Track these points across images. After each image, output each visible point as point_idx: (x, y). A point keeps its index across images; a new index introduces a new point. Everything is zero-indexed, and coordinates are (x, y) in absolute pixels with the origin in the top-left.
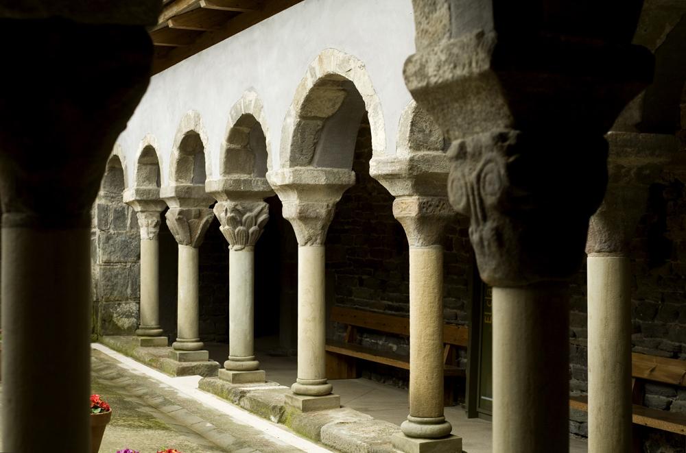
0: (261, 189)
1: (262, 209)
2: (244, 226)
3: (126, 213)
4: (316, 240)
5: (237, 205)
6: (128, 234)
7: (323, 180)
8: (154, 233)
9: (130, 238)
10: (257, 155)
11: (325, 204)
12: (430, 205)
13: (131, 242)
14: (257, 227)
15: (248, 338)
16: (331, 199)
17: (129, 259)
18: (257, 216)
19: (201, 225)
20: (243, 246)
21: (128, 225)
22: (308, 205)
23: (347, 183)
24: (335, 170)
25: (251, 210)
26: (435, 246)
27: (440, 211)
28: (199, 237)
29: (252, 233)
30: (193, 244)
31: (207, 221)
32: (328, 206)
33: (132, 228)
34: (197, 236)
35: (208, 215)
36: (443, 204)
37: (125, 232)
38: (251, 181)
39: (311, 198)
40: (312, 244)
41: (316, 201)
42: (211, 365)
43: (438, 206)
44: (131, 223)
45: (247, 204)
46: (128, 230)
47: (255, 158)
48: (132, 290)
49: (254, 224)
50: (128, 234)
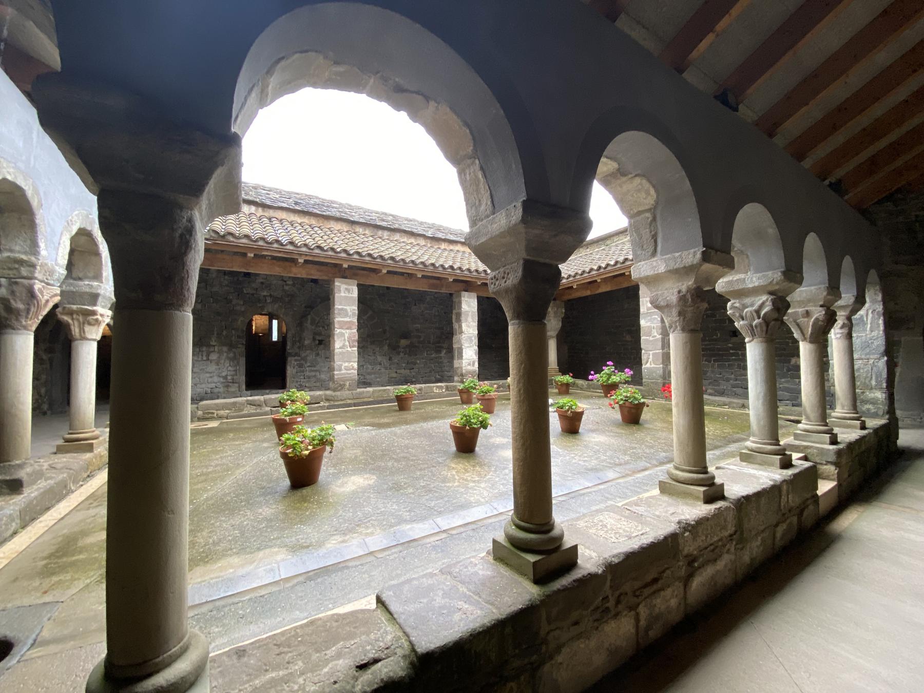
0: (756, 284)
1: (763, 304)
2: (747, 320)
3: (865, 319)
4: (676, 327)
5: (735, 303)
6: (868, 336)
7: (663, 268)
8: (842, 333)
9: (871, 339)
10: (749, 254)
11: (676, 290)
13: (872, 343)
14: (761, 319)
15: (762, 423)
16: (683, 285)
17: (872, 357)
18: (758, 312)
19: (811, 323)
20: (751, 339)
21: (868, 329)
22: (657, 294)
23: (690, 264)
24: (677, 254)
25: (752, 305)
27: (505, 282)
28: (811, 333)
29: (756, 326)
30: (808, 340)
31: (817, 319)
32: (679, 292)
33: (872, 331)
34: (809, 333)
35: (817, 313)
37: (864, 335)
38: (744, 279)
39: (660, 288)
40: (674, 331)
41: (666, 289)
44: (871, 327)
45: (747, 301)
46: (868, 333)
47: (747, 257)
48: (876, 382)
49: (756, 317)
50: (868, 336)
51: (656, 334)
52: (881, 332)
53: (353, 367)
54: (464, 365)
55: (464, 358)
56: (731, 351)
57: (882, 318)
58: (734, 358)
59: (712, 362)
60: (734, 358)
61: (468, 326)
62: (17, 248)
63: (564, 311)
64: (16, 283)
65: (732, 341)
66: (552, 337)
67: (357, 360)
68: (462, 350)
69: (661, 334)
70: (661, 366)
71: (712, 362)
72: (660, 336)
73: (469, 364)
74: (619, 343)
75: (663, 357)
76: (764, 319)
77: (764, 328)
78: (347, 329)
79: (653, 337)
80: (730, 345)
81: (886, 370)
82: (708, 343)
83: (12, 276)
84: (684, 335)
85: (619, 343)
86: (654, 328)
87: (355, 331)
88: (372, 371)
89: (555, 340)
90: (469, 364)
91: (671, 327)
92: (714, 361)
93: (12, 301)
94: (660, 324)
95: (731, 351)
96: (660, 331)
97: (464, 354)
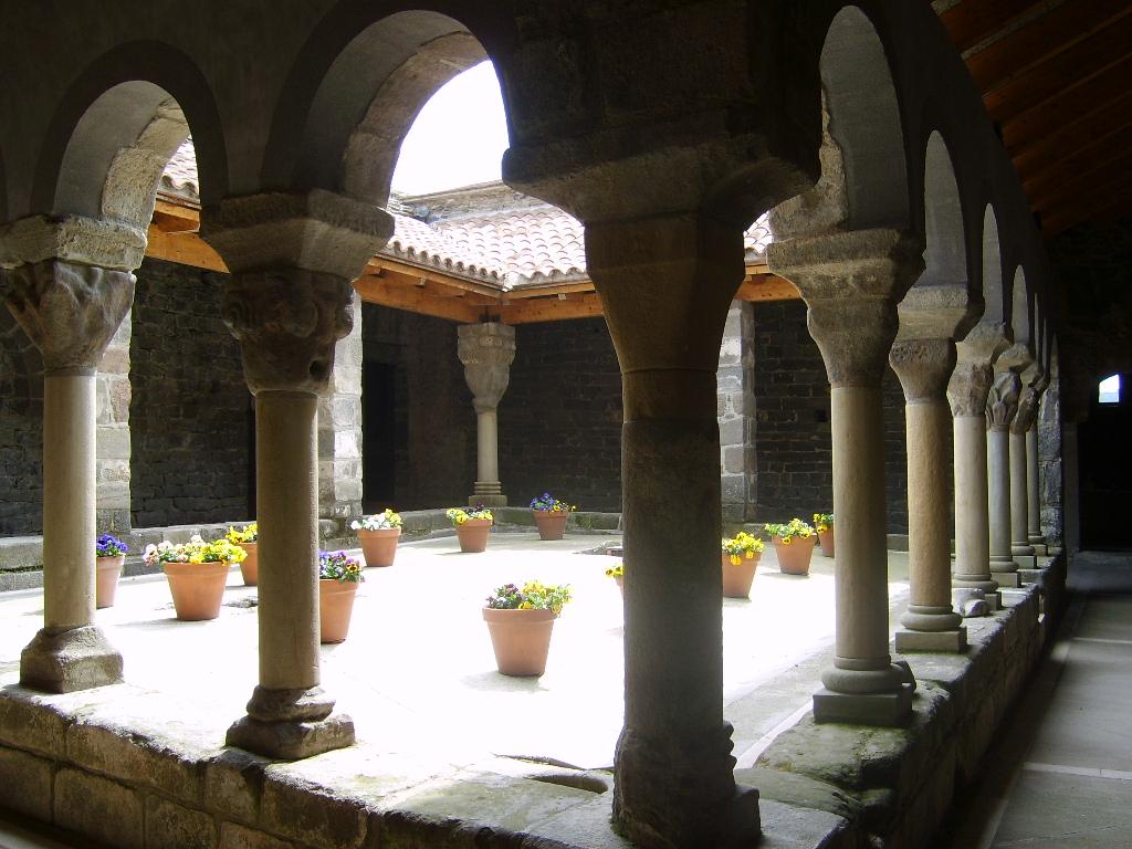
1: (1005, 381)
12: (906, 353)
26: (925, 399)
29: (996, 410)
32: (974, 368)
36: (925, 349)
42: (1030, 573)
43: (916, 352)
49: (996, 399)
51: (732, 412)
52: (1056, 423)
53: (122, 472)
54: (336, 473)
55: (337, 454)
56: (817, 450)
57: (1058, 402)
58: (820, 462)
59: (784, 471)
60: (820, 462)
61: (345, 376)
62: (124, 213)
63: (514, 347)
64: (116, 278)
65: (819, 430)
66: (487, 408)
67: (129, 454)
68: (333, 434)
69: (743, 412)
70: (742, 474)
71: (784, 471)
72: (742, 416)
73: (346, 472)
74: (596, 428)
75: (745, 455)
76: (1004, 402)
77: (1004, 414)
78: (110, 371)
79: (727, 417)
80: (815, 438)
81: (1060, 476)
82: (776, 432)
83: (111, 266)
84: (974, 418)
85: (596, 428)
86: (729, 400)
87: (125, 376)
88: (14, 491)
89: (495, 415)
90: (346, 472)
91: (958, 408)
92: (787, 470)
93: (105, 313)
94: (741, 392)
95: (817, 450)
96: (740, 407)
97: (336, 446)
